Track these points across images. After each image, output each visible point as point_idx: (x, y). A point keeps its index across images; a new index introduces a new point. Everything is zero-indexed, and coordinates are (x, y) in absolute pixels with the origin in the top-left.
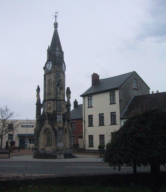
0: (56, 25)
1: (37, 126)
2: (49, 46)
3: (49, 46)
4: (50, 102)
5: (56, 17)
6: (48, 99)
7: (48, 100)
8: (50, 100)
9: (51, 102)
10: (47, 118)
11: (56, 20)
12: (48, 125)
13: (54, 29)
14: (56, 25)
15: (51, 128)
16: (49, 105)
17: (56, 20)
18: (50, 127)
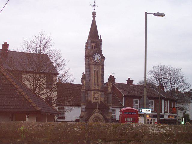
0: (94, 14)
1: (85, 113)
4: (98, 92)
5: (94, 6)
6: (98, 89)
7: (94, 90)
8: (98, 90)
10: (97, 107)
11: (94, 9)
12: (99, 114)
13: (92, 19)
14: (94, 14)
15: (103, 117)
16: (96, 95)
17: (94, 9)
18: (101, 115)
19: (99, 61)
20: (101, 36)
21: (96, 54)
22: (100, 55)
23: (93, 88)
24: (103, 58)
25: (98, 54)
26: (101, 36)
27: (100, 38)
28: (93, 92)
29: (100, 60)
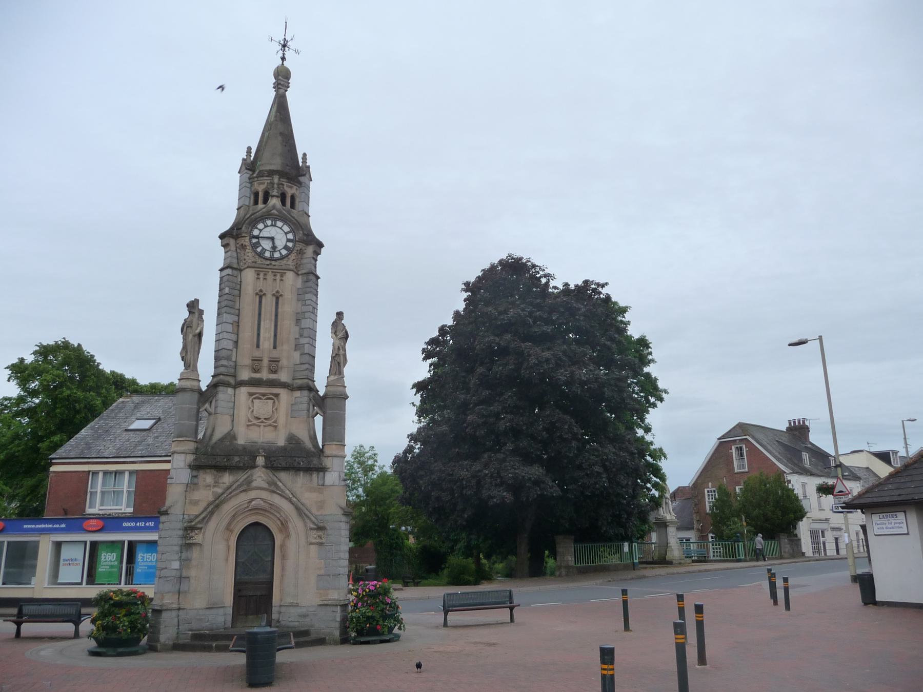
0: (282, 78)
2: (249, 149)
3: (249, 149)
9: (277, 395)
11: (283, 59)
14: (282, 78)
16: (263, 408)
17: (283, 59)
19: (284, 252)
20: (305, 155)
21: (269, 222)
22: (286, 228)
23: (245, 375)
24: (308, 243)
25: (279, 224)
26: (305, 155)
27: (301, 164)
28: (244, 390)
29: (286, 247)
